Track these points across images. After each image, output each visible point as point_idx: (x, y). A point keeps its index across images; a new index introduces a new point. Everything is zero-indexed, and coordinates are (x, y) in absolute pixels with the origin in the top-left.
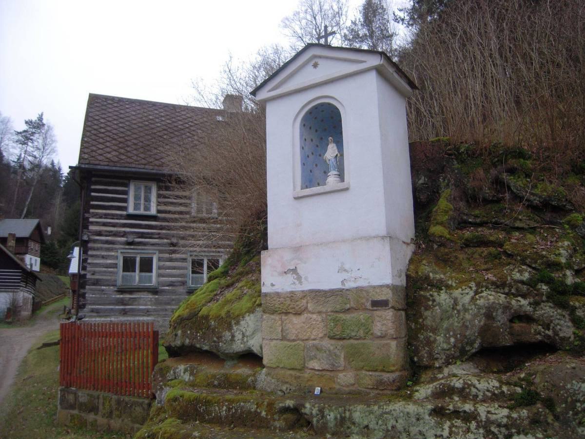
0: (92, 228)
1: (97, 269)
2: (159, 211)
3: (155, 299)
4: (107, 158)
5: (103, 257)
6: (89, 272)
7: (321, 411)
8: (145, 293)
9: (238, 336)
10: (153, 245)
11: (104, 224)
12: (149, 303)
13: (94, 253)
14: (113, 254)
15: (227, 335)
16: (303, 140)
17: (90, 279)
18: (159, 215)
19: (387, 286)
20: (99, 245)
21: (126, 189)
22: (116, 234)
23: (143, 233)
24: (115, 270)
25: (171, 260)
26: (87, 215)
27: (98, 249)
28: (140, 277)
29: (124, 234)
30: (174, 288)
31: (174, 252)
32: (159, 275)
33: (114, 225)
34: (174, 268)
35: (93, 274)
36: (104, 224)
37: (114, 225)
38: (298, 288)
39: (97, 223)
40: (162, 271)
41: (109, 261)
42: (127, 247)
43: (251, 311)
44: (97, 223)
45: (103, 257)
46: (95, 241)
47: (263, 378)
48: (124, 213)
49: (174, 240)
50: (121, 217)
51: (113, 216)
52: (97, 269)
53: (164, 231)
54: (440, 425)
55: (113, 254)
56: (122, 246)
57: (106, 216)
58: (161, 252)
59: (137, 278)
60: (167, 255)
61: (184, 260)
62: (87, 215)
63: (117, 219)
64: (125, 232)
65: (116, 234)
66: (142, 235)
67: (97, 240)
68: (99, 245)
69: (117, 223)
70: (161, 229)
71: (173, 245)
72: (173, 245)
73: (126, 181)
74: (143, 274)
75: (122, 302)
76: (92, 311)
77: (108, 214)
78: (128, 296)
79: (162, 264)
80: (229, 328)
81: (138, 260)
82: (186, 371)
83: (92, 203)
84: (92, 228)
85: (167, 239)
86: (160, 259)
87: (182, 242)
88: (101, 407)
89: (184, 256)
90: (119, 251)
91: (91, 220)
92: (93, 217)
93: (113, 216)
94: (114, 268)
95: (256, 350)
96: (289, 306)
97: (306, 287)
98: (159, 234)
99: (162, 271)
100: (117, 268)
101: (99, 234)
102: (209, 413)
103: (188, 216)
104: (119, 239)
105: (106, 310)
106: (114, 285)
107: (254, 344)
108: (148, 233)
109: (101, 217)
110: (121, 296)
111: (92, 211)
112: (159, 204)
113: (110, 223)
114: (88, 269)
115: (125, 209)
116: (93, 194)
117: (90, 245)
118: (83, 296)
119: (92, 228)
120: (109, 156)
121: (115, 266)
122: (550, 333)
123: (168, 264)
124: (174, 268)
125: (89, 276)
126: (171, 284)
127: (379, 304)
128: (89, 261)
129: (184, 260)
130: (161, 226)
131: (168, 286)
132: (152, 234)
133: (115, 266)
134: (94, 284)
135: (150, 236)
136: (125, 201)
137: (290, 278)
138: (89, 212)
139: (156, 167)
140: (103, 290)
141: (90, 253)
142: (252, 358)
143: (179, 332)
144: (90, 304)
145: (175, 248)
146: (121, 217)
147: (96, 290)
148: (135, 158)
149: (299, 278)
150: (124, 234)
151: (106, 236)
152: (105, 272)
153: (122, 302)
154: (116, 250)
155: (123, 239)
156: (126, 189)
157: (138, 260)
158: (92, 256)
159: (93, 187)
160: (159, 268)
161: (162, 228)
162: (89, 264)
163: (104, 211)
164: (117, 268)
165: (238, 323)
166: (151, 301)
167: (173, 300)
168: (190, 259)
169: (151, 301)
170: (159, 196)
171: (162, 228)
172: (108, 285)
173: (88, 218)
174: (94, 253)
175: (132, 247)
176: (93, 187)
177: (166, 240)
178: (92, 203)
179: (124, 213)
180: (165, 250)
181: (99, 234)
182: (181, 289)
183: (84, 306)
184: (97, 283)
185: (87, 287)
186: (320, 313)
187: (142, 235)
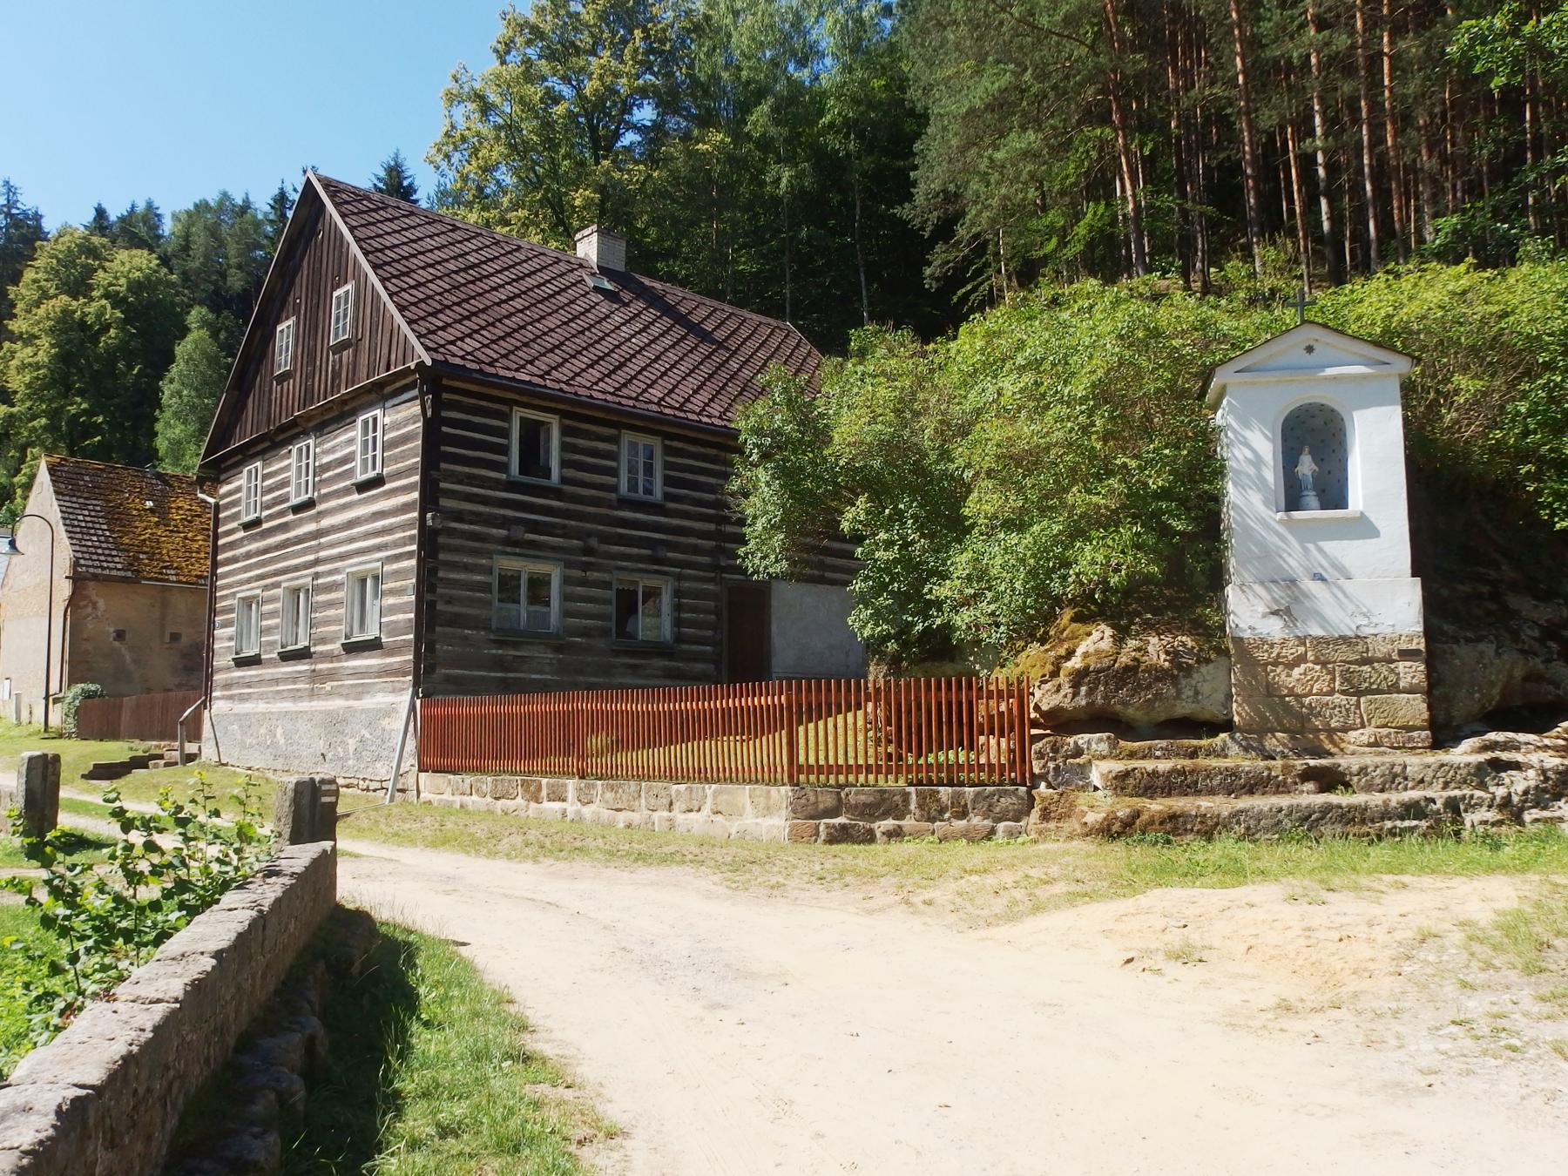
2: (564, 480)
3: (559, 660)
5: (467, 568)
10: (554, 548)
11: (469, 498)
12: (547, 669)
18: (566, 487)
25: (584, 583)
26: (434, 474)
28: (529, 613)
29: (504, 522)
31: (586, 567)
32: (566, 614)
33: (485, 501)
35: (448, 603)
36: (469, 498)
37: (485, 501)
42: (509, 549)
49: (594, 542)
52: (454, 592)
57: (471, 480)
58: (568, 565)
59: (524, 615)
66: (534, 527)
72: (588, 551)
73: (505, 408)
74: (533, 608)
75: (499, 664)
76: (448, 679)
79: (569, 589)
83: (443, 448)
86: (566, 581)
87: (605, 547)
91: (442, 485)
98: (564, 527)
101: (459, 516)
103: (613, 495)
104: (494, 531)
105: (474, 678)
106: (488, 628)
109: (460, 483)
111: (443, 465)
113: (477, 495)
115: (503, 467)
116: (444, 429)
117: (441, 540)
119: (445, 502)
122: (1561, 692)
126: (585, 632)
127: (1406, 655)
128: (441, 574)
133: (486, 587)
136: (505, 450)
138: (438, 469)
140: (466, 638)
141: (442, 556)
145: (592, 559)
150: (504, 522)
153: (499, 664)
154: (489, 554)
156: (505, 425)
160: (566, 598)
163: (467, 469)
173: (436, 482)
176: (444, 414)
178: (443, 448)
179: (504, 476)
182: (601, 644)
185: (438, 629)
187: (534, 527)
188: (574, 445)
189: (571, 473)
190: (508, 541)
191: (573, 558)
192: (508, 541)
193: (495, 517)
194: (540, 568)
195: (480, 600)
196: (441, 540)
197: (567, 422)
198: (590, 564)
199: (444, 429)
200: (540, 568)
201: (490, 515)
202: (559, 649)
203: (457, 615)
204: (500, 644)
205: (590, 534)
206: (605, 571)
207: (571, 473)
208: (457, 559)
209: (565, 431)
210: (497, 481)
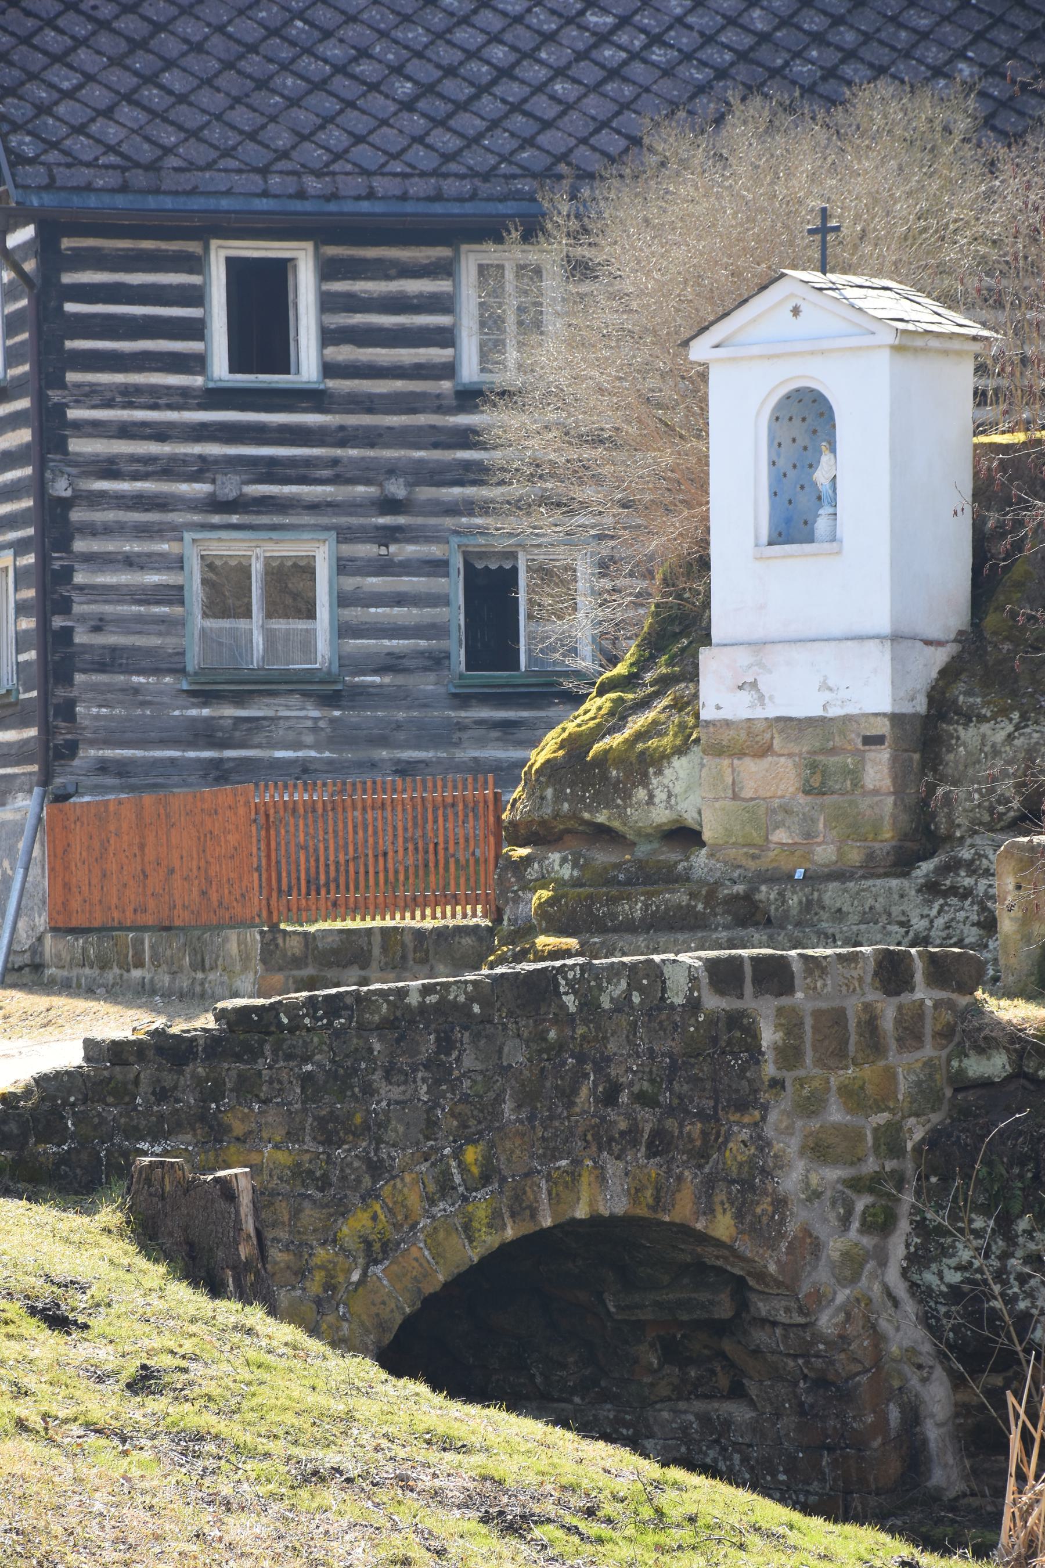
0: (78, 446)
1: (108, 609)
2: (329, 369)
4: (110, 149)
5: (130, 562)
6: (83, 619)
7: (781, 894)
8: (295, 699)
9: (660, 796)
10: (314, 507)
11: (126, 431)
12: (309, 739)
13: (95, 546)
14: (165, 547)
15: (641, 794)
16: (775, 445)
17: (86, 648)
18: (331, 384)
19: (885, 715)
20: (111, 516)
21: (195, 279)
22: (169, 469)
23: (272, 461)
24: (178, 610)
25: (385, 567)
26: (55, 396)
27: (107, 531)
28: (270, 637)
29: (203, 469)
30: (400, 680)
31: (389, 535)
32: (344, 630)
33: (161, 433)
34: (399, 600)
35: (97, 629)
36: (126, 431)
37: (161, 433)
38: (759, 713)
39: (96, 430)
40: (354, 614)
41: (153, 578)
42: (216, 519)
43: (681, 751)
44: (96, 430)
45: (130, 562)
46: (97, 499)
47: (700, 859)
48: (198, 381)
49: (397, 489)
50: (183, 398)
51: (155, 397)
52: (108, 609)
53: (353, 452)
54: (929, 903)
55: (165, 547)
56: (197, 518)
57: (130, 397)
58: (345, 536)
59: (258, 640)
60: (367, 550)
61: (438, 567)
62: (55, 396)
63: (170, 407)
64: (202, 458)
65: (169, 469)
66: (270, 471)
67: (103, 494)
68: (111, 516)
69: (172, 425)
70: (342, 444)
71: (390, 505)
72: (390, 505)
73: (193, 247)
74: (280, 625)
75: (206, 734)
76: (103, 767)
77: (138, 389)
78: (230, 711)
79: (350, 583)
80: (644, 781)
81: (257, 568)
82: (564, 860)
83: (69, 344)
84: (79, 446)
85: (368, 482)
86: (343, 567)
87: (426, 493)
88: (376, 951)
89: (435, 551)
90: (188, 536)
91: (73, 414)
92: (78, 403)
93: (155, 397)
94: (169, 603)
95: (690, 818)
96: (752, 741)
97: (772, 711)
98: (335, 462)
99: (354, 614)
100: (182, 602)
101: (109, 468)
102: (613, 916)
104: (184, 488)
107: (688, 809)
108: (292, 462)
109: (109, 404)
110: (206, 712)
111: (72, 377)
112: (328, 337)
113: (144, 424)
114: (77, 609)
115: (197, 363)
116: (70, 307)
117: (77, 515)
118: (67, 710)
119: (78, 446)
120: (112, 133)
121: (175, 595)
123: (374, 583)
124: (399, 600)
125: (81, 637)
126: (391, 664)
128: (79, 578)
129: (438, 567)
130: (342, 428)
131: (376, 671)
132: (308, 462)
133: (175, 595)
134: (102, 667)
135: (300, 472)
136: (196, 330)
137: (746, 697)
138: (62, 385)
139: (312, 184)
140: (136, 690)
141: (80, 545)
142: (685, 836)
143: (549, 792)
144: (93, 743)
145: (401, 520)
146: (183, 398)
147: (110, 689)
148: (216, 133)
149: (761, 698)
150: (203, 468)
151: (135, 477)
152: (139, 619)
154: (174, 532)
155: (201, 489)
156: (195, 279)
157: (257, 568)
158: (89, 558)
159: (68, 278)
160: (342, 600)
161: (343, 437)
162: (81, 588)
163: (119, 378)
164: (182, 602)
165: (659, 772)
166: (315, 729)
167: (399, 726)
168: (458, 563)
169: (315, 729)
170: (327, 303)
171: (343, 437)
172: (156, 671)
173: (60, 409)
174: (95, 546)
175: (235, 519)
176: (68, 278)
177: (361, 489)
178: (69, 344)
179: (198, 381)
180: (363, 529)
181: (109, 468)
182: (427, 684)
183: (72, 749)
184: (111, 661)
185: (79, 678)
186: (790, 755)
187: (270, 471)
188: (350, 295)
189: (345, 353)
190: (216, 505)
191: (354, 521)
192: (216, 505)
193: (184, 460)
194: (289, 548)
195: (162, 620)
196: (77, 515)
197: (332, 251)
198: (398, 529)
199: (70, 307)
200: (289, 548)
201: (173, 458)
202: (330, 699)
203: (114, 650)
204: (205, 696)
205: (392, 470)
206: (428, 540)
207: (345, 353)
208: (109, 546)
209: (328, 270)
210: (185, 392)
